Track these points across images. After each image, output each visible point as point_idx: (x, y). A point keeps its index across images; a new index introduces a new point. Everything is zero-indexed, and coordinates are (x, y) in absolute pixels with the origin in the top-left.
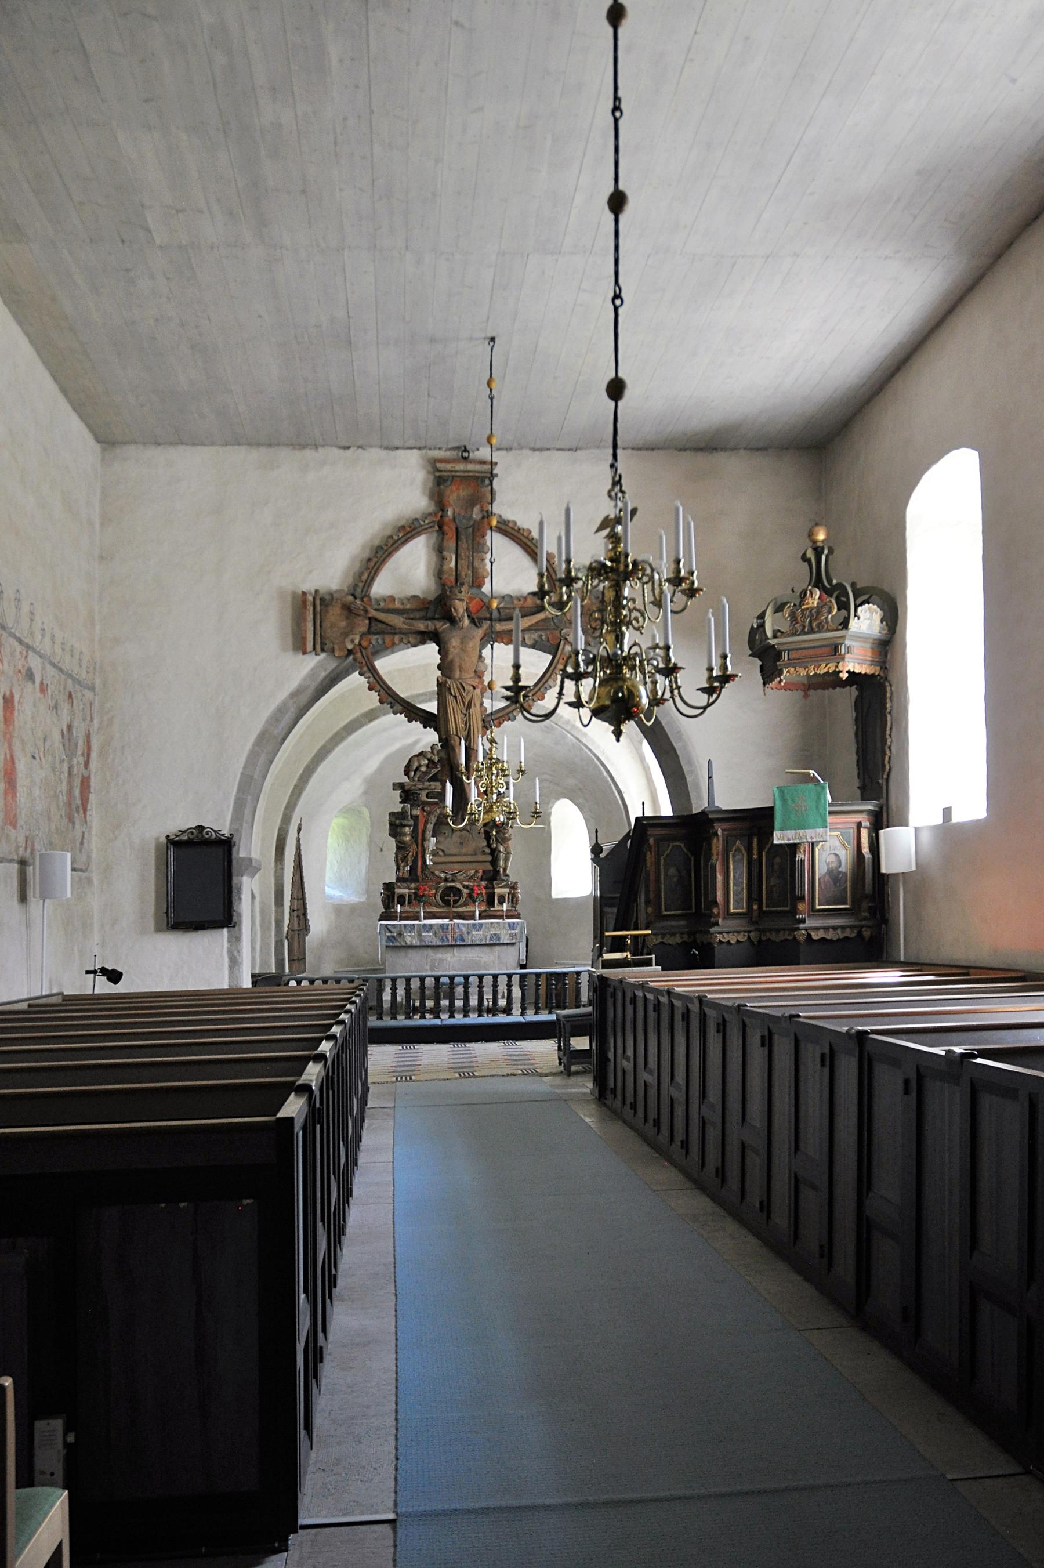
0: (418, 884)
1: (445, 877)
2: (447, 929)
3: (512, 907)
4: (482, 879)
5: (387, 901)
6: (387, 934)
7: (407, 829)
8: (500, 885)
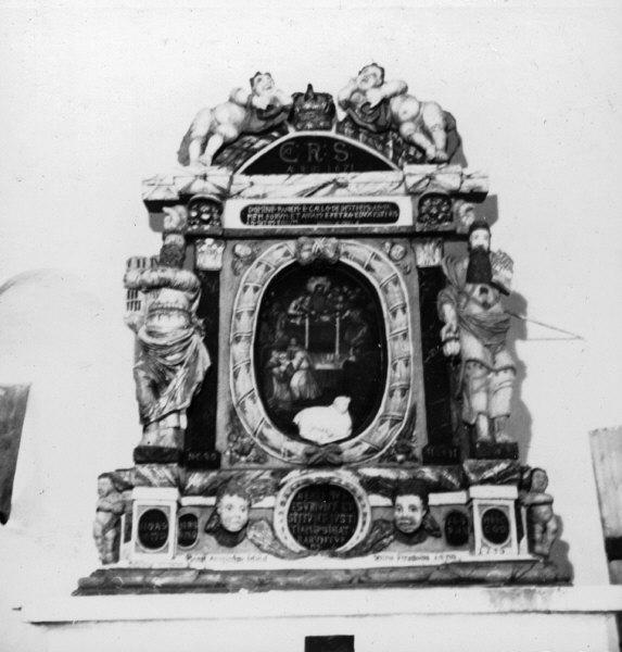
0: (213, 474)
3: (531, 549)
4: (428, 460)
5: (110, 534)
8: (488, 474)
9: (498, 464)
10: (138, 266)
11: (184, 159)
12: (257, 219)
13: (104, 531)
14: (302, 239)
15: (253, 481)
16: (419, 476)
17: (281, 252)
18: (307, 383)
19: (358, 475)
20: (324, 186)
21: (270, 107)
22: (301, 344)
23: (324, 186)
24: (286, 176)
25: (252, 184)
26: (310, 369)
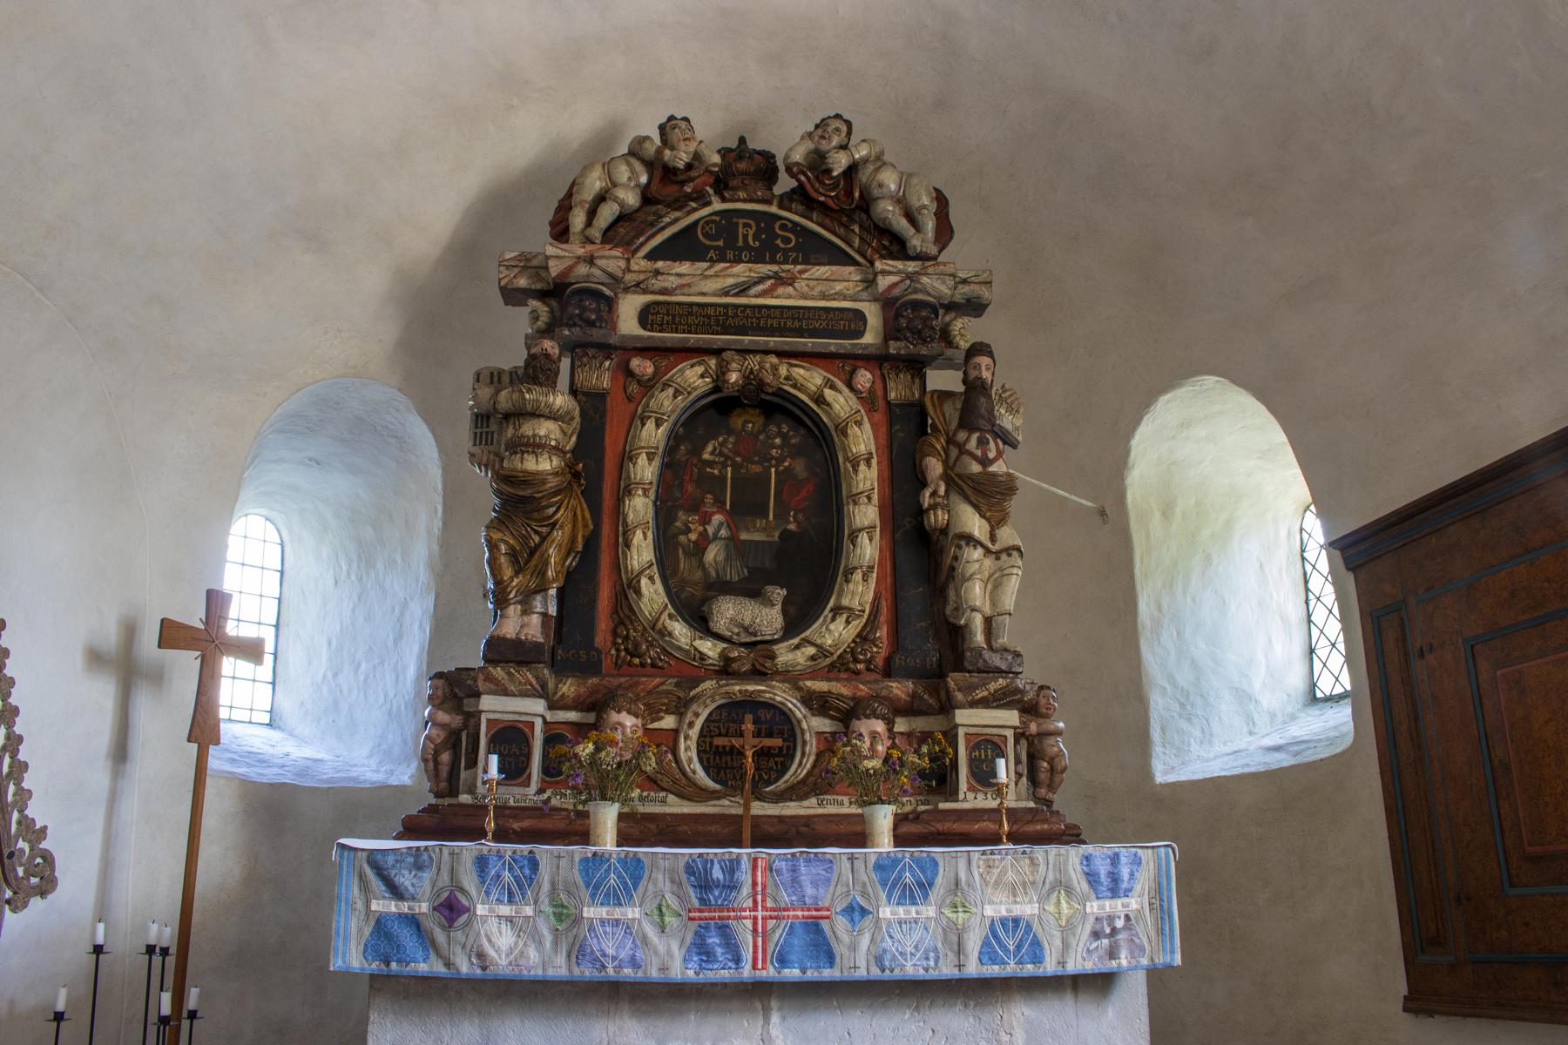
0: (593, 681)
1: (724, 656)
2: (733, 886)
4: (888, 672)
5: (445, 757)
6: (375, 906)
7: (547, 429)
9: (996, 680)
10: (492, 382)
11: (561, 232)
12: (662, 325)
13: (436, 753)
14: (728, 354)
15: (650, 693)
16: (884, 693)
17: (700, 370)
18: (728, 558)
19: (799, 689)
20: (761, 280)
21: (689, 167)
22: (720, 502)
23: (761, 280)
24: (705, 265)
25: (657, 273)
26: (733, 540)
